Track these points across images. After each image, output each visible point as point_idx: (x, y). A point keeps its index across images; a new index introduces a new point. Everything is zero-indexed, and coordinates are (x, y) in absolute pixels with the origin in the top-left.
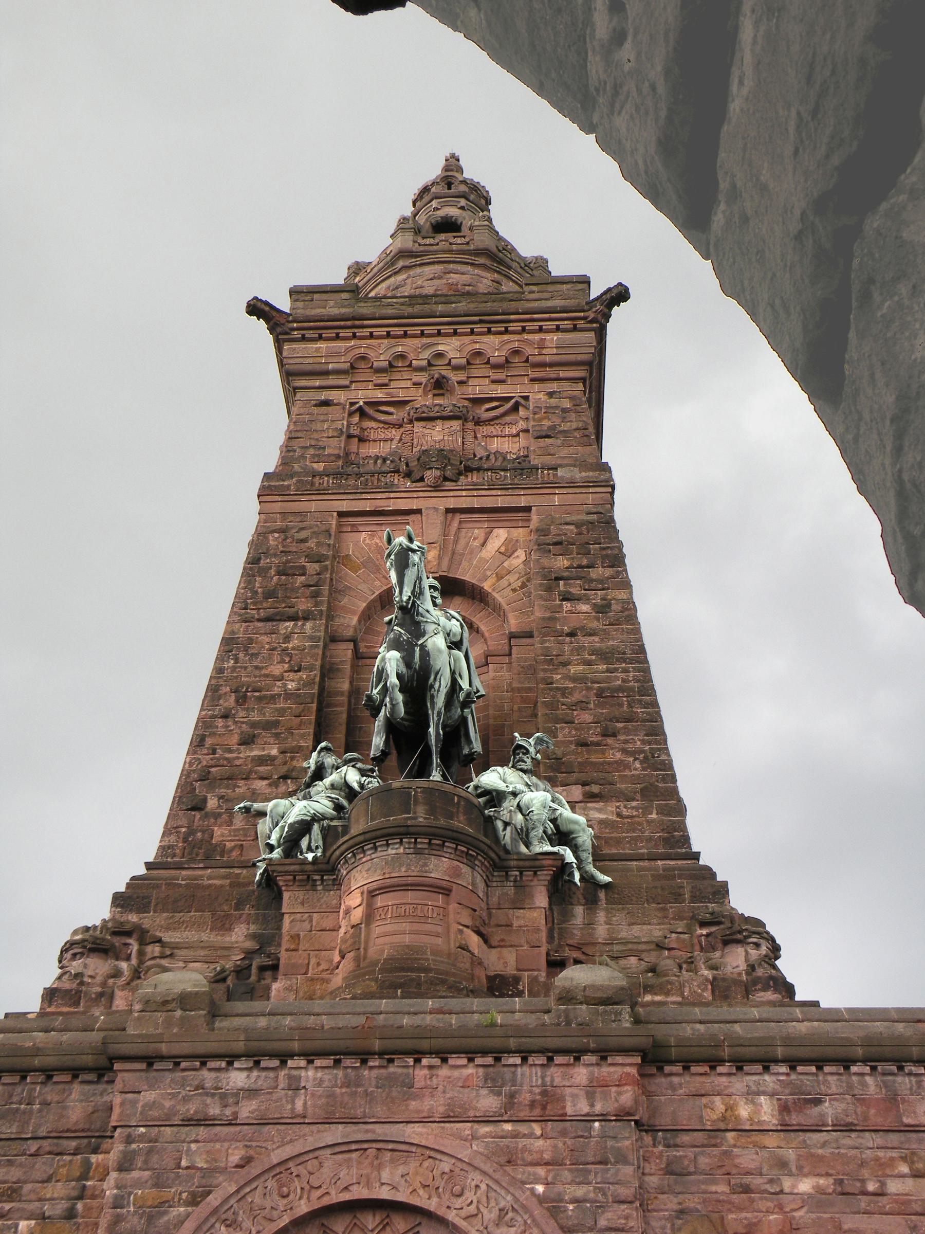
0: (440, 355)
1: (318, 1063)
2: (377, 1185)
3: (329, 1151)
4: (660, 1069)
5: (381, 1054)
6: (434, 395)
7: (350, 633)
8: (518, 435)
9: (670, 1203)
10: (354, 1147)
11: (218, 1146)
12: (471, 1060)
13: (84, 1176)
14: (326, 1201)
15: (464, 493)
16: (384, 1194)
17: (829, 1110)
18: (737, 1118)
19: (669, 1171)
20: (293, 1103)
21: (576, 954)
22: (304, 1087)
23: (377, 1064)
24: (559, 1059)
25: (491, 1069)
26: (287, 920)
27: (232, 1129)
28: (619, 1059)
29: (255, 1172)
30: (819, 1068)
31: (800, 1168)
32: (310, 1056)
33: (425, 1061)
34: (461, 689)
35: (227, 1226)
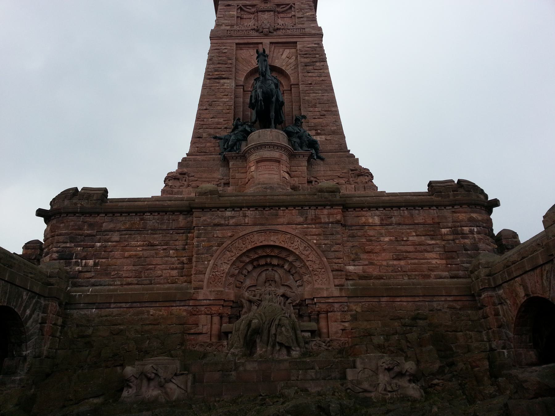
1: (251, 209)
2: (270, 241)
3: (255, 233)
4: (347, 210)
5: (269, 207)
6: (264, 3)
7: (242, 83)
8: (291, 17)
9: (350, 244)
10: (263, 231)
11: (224, 231)
12: (295, 208)
13: (187, 239)
14: (256, 245)
15: (276, 37)
16: (272, 243)
17: (394, 220)
18: (369, 223)
19: (349, 236)
20: (245, 220)
21: (315, 179)
22: (248, 216)
23: (268, 209)
24: (319, 208)
25: (300, 211)
26: (231, 171)
27: (227, 227)
28: (337, 207)
29: (236, 238)
30: (392, 209)
31: (386, 235)
32: (249, 208)
33: (281, 209)
34: (280, 101)
35: (229, 252)
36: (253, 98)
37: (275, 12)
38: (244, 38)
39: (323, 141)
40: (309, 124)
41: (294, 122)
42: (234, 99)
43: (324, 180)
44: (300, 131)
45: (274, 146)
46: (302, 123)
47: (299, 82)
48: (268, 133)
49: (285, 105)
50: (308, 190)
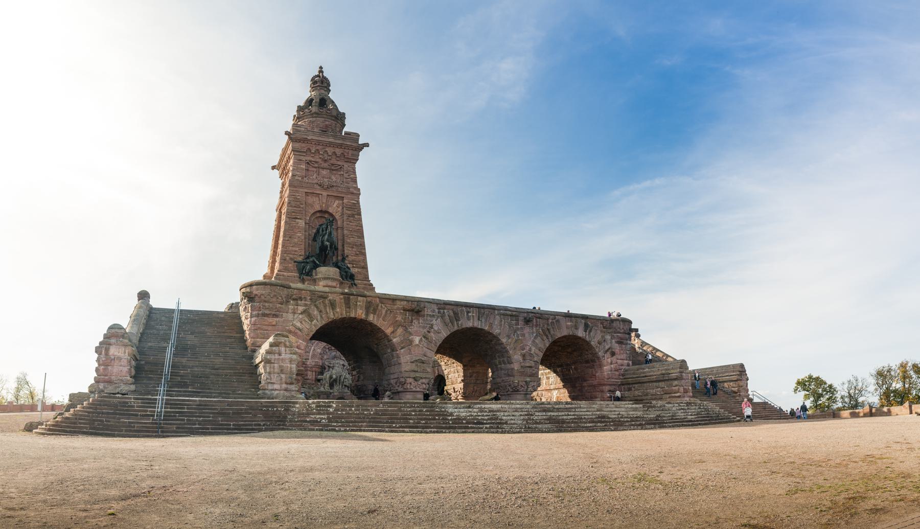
0: (326, 151)
7: (308, 222)
37: (330, 169)
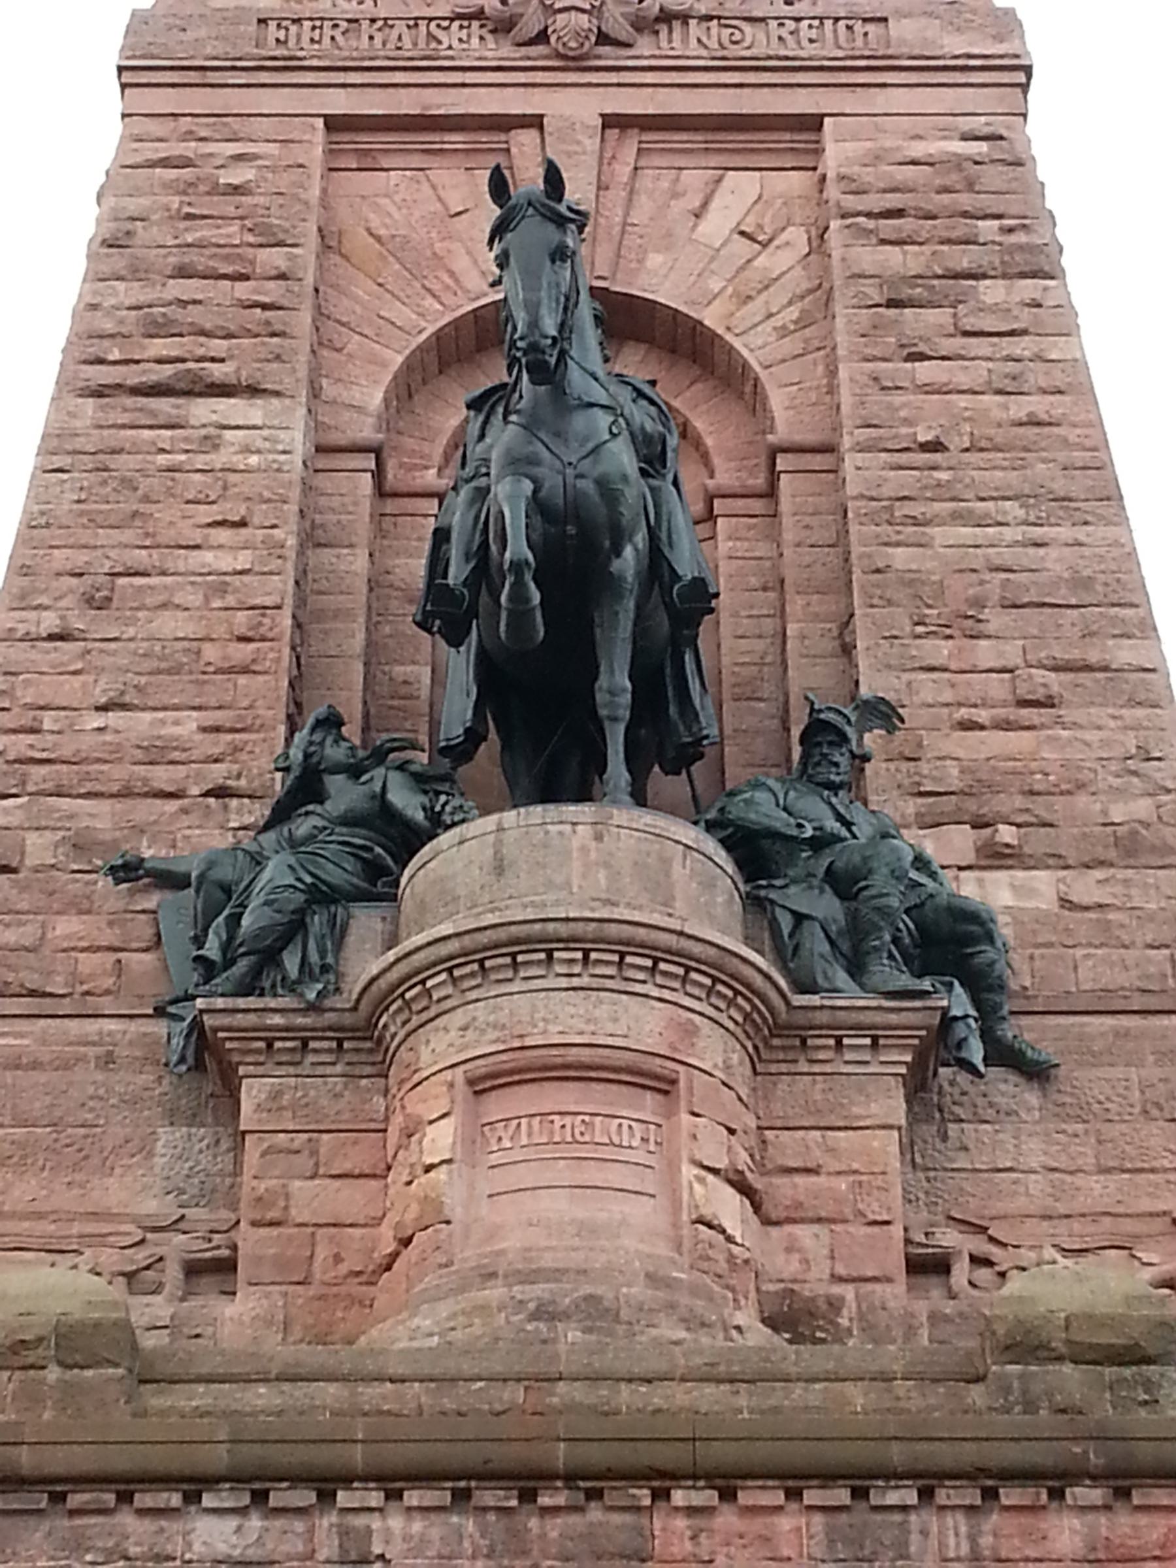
36: (455, 552)
38: (399, 77)
39: (1041, 918)
40: (925, 768)
41: (797, 752)
42: (301, 552)
43: (1049, 1253)
44: (848, 825)
45: (623, 949)
46: (866, 758)
47: (837, 428)
48: (575, 843)
49: (724, 617)
50: (911, 1332)
